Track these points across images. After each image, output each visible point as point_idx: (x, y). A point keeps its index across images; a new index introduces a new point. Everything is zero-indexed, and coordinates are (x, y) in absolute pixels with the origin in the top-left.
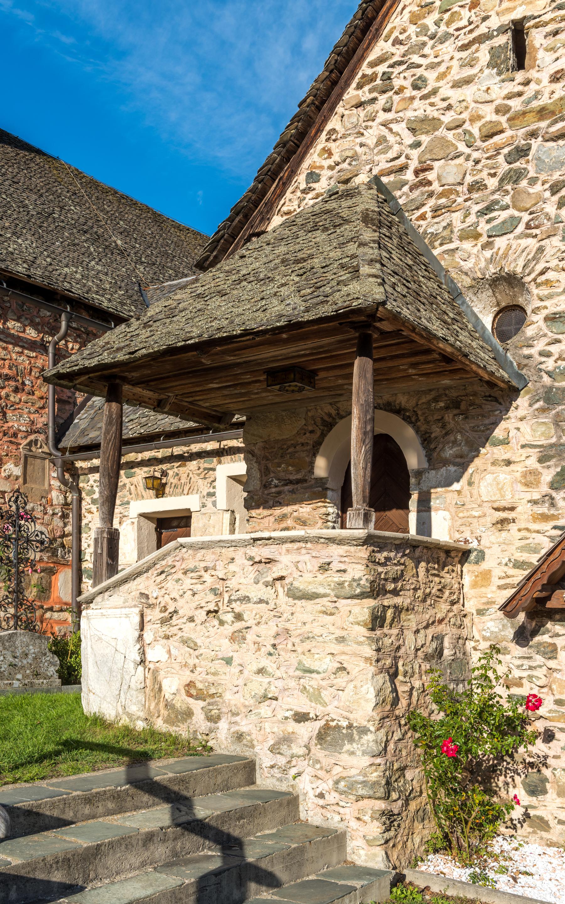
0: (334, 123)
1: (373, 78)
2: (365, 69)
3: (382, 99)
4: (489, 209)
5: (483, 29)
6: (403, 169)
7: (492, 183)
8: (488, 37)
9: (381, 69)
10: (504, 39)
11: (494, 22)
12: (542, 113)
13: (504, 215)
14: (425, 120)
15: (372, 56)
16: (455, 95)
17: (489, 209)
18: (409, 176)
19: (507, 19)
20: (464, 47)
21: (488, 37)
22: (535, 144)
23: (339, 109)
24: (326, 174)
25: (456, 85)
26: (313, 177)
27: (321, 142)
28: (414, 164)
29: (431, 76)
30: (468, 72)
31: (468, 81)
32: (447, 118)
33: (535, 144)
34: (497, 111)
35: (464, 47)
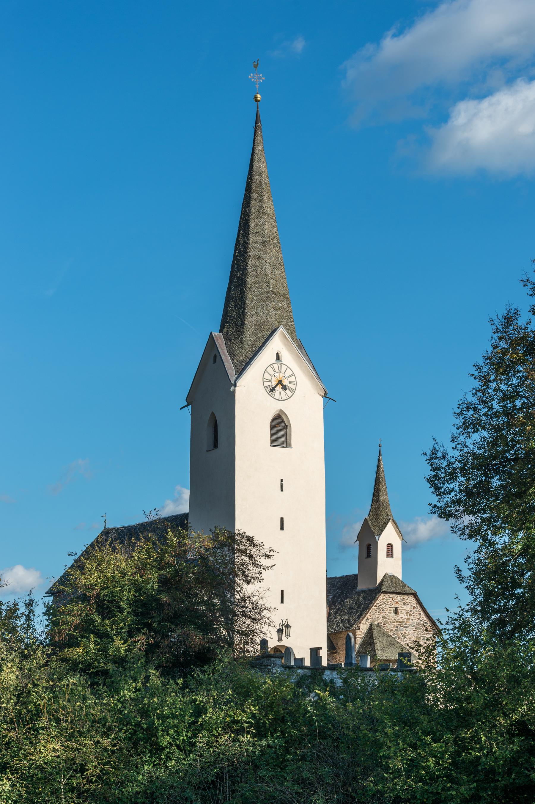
0: (370, 611)
1: (376, 606)
2: (375, 604)
3: (378, 610)
4: (394, 634)
5: (392, 606)
6: (382, 623)
7: (394, 630)
8: (392, 608)
9: (378, 605)
10: (395, 609)
11: (394, 606)
12: (400, 622)
13: (395, 636)
14: (385, 617)
15: (377, 602)
16: (388, 614)
17: (394, 634)
18: (382, 624)
19: (396, 606)
20: (390, 608)
21: (392, 608)
22: (399, 626)
23: (372, 609)
24: (370, 620)
25: (389, 613)
26: (368, 619)
27: (369, 614)
28: (383, 623)
29: (385, 610)
30: (390, 612)
31: (390, 613)
32: (388, 618)
33: (399, 626)
34: (394, 619)
35: (390, 608)
